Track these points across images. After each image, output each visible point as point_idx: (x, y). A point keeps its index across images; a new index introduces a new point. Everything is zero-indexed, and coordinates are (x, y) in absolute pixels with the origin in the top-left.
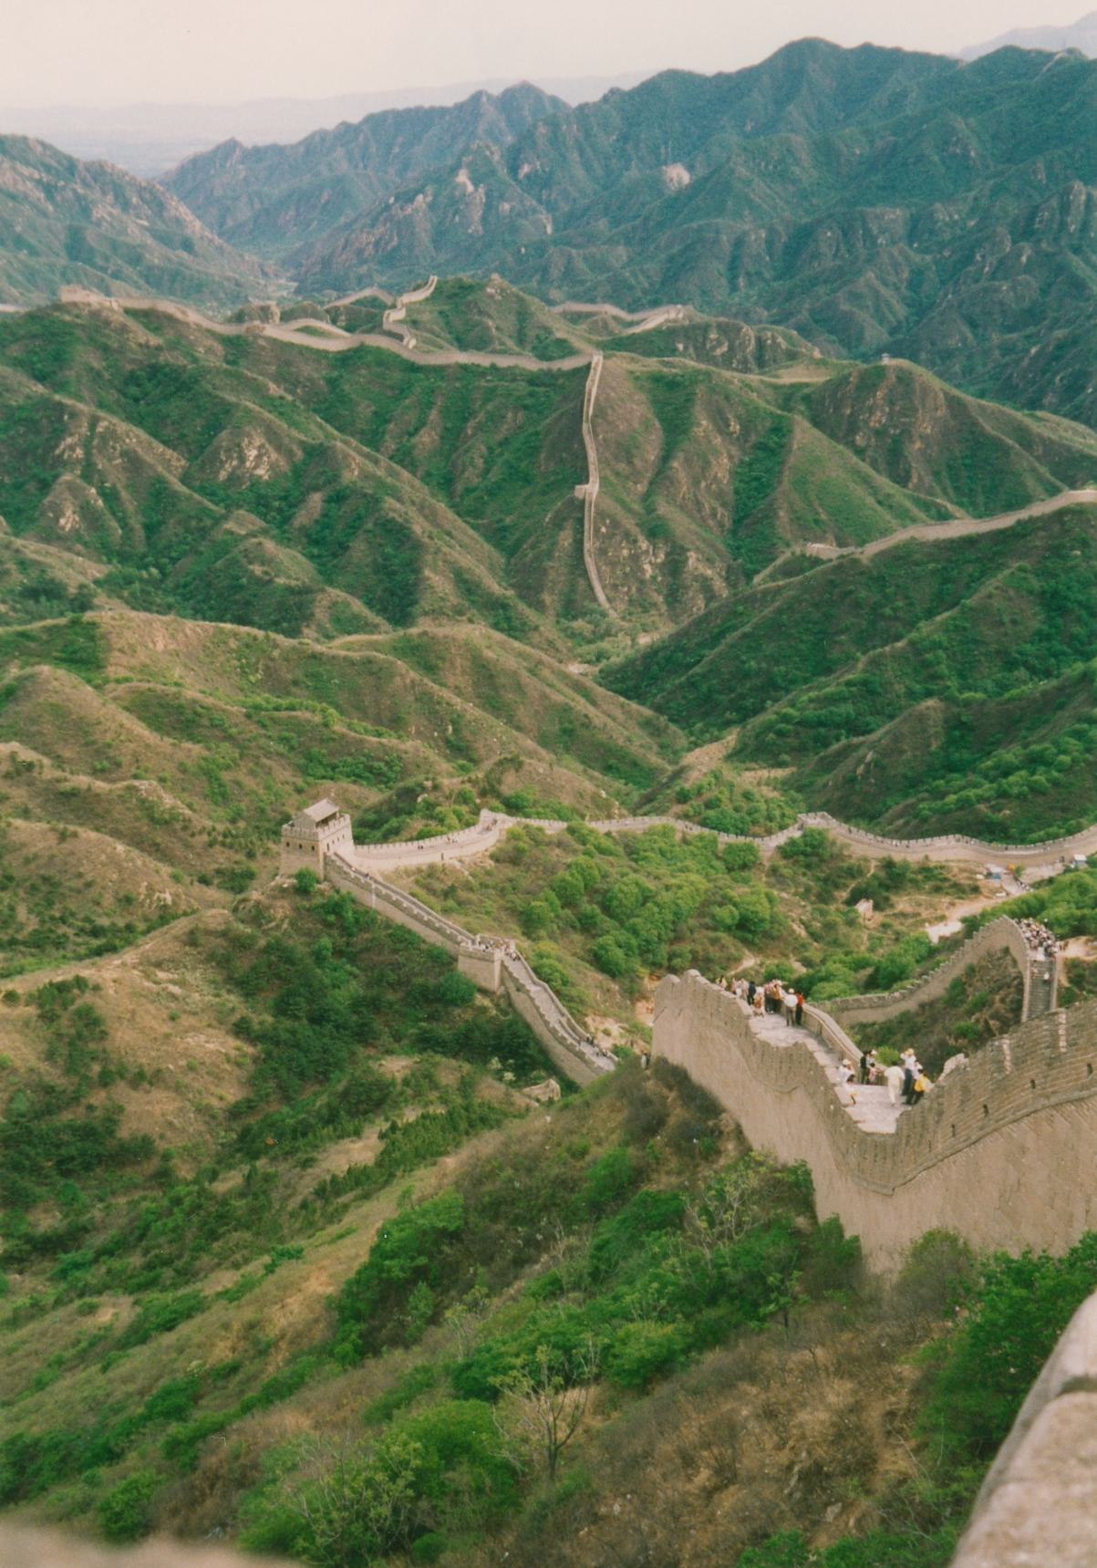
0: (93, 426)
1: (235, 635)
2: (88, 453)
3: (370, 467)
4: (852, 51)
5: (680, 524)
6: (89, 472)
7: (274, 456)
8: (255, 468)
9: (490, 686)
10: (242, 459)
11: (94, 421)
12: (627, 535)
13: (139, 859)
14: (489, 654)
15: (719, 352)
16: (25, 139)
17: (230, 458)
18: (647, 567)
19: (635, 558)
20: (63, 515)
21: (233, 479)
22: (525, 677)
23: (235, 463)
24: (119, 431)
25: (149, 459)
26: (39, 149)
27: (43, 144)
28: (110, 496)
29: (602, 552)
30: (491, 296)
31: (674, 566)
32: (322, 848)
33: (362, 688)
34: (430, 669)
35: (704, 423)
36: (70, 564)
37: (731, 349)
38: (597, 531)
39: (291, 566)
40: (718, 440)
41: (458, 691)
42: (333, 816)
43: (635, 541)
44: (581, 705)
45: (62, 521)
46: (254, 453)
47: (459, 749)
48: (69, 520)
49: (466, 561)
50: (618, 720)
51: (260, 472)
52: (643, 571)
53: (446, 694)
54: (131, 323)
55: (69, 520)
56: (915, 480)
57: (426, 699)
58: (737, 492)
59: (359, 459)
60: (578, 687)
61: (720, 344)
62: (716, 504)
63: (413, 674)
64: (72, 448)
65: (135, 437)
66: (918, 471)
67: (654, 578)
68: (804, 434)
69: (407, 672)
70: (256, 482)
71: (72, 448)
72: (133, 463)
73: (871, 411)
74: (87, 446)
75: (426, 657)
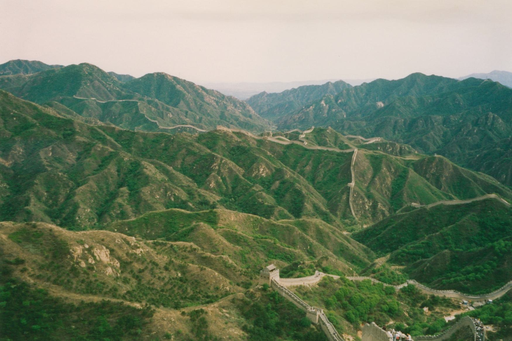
0: (221, 161)
1: (253, 217)
3: (292, 175)
4: (429, 76)
5: (377, 195)
6: (219, 173)
7: (267, 171)
9: (321, 236)
10: (259, 171)
11: (222, 159)
12: (362, 197)
13: (221, 277)
14: (321, 227)
15: (389, 150)
16: (213, 90)
17: (256, 171)
18: (367, 206)
19: (364, 204)
21: (256, 176)
22: (331, 234)
25: (235, 170)
27: (217, 92)
28: (224, 179)
29: (354, 201)
31: (374, 207)
32: (271, 278)
33: (286, 234)
36: (211, 196)
37: (393, 149)
38: (353, 195)
39: (269, 199)
40: (388, 174)
41: (312, 237)
42: (274, 269)
43: (364, 199)
44: (346, 243)
46: (262, 170)
47: (311, 253)
48: (212, 185)
49: (316, 201)
50: (356, 248)
51: (263, 175)
52: (366, 207)
53: (308, 237)
54: (234, 135)
55: (212, 185)
56: (443, 188)
57: (302, 238)
58: (393, 188)
59: (290, 173)
60: (346, 238)
61: (390, 148)
62: (386, 190)
63: (299, 231)
64: (215, 166)
65: (232, 164)
66: (444, 185)
67: (368, 209)
69: (298, 231)
70: (262, 177)
71: (215, 166)
72: (231, 171)
73: (431, 168)
74: (219, 166)
75: (304, 227)
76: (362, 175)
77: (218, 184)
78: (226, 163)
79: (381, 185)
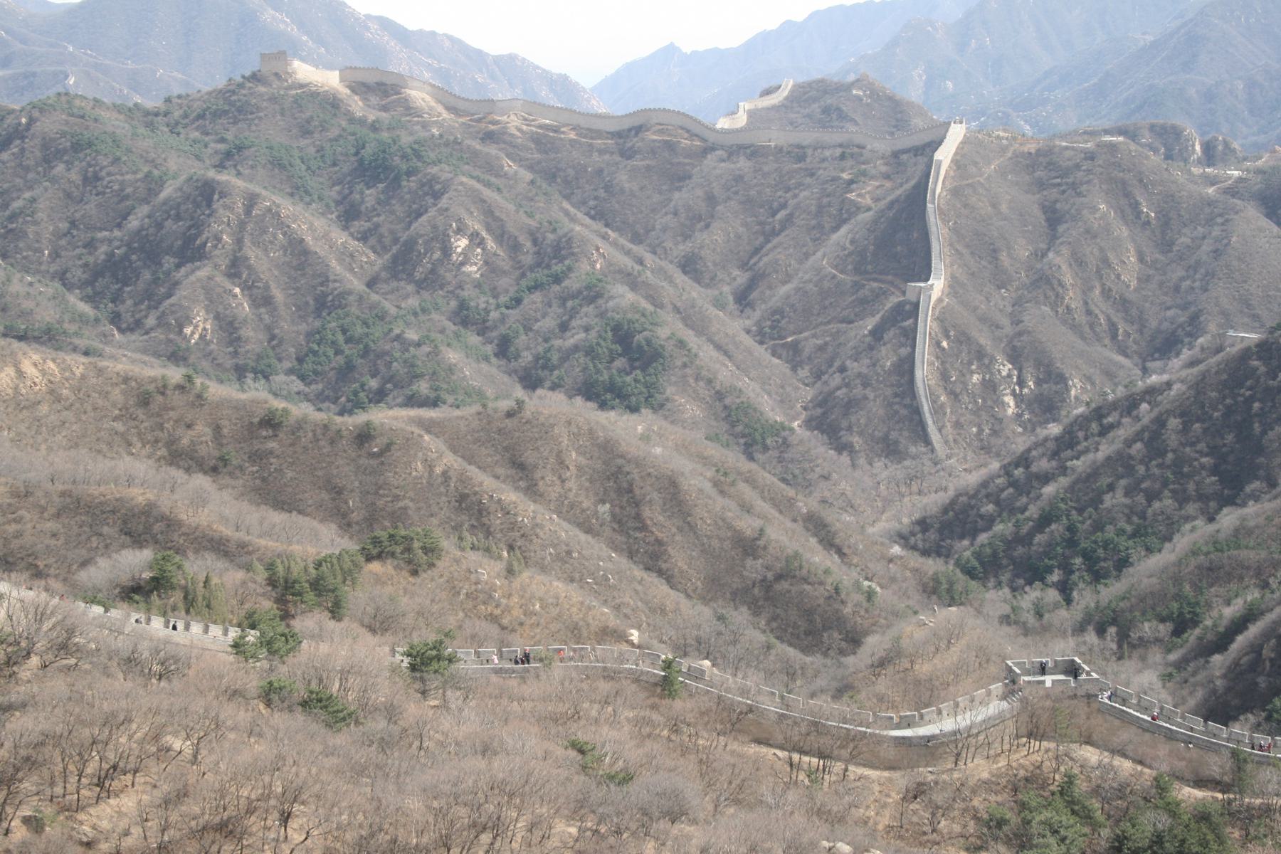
1: (126, 380)
2: (239, 242)
3: (628, 262)
5: (1060, 342)
6: (236, 268)
7: (491, 244)
8: (462, 264)
10: (447, 250)
11: (251, 200)
12: (980, 354)
16: (433, 34)
19: (990, 387)
20: (188, 320)
23: (437, 255)
24: (283, 212)
26: (447, 44)
27: (450, 38)
28: (263, 301)
30: (859, 99)
34: (521, 471)
35: (1102, 206)
41: (567, 510)
44: (784, 536)
45: (188, 331)
48: (200, 325)
49: (725, 373)
52: (1004, 405)
55: (200, 325)
59: (604, 248)
62: (1117, 318)
67: (1019, 416)
68: (1252, 222)
72: (298, 253)
76: (982, 249)
77: (229, 327)
78: (274, 213)
79: (1087, 290)
